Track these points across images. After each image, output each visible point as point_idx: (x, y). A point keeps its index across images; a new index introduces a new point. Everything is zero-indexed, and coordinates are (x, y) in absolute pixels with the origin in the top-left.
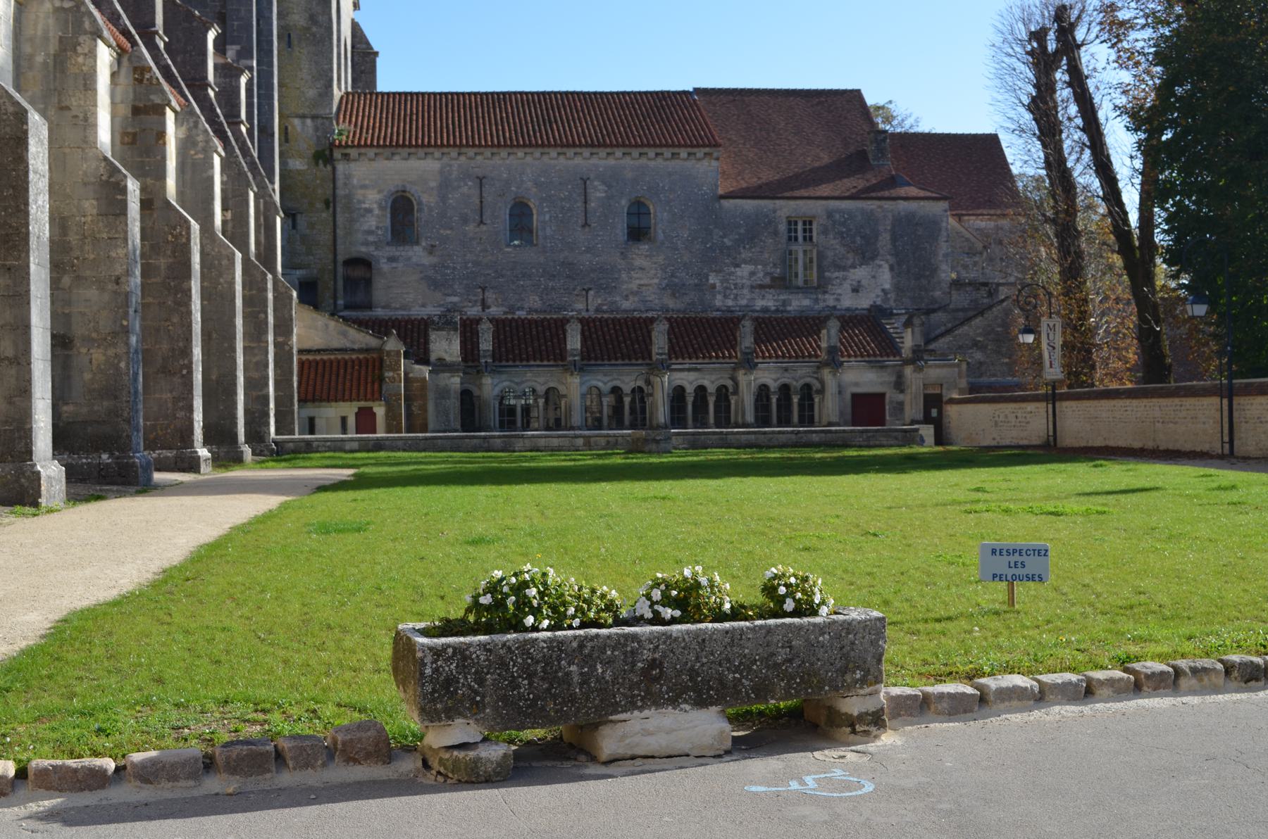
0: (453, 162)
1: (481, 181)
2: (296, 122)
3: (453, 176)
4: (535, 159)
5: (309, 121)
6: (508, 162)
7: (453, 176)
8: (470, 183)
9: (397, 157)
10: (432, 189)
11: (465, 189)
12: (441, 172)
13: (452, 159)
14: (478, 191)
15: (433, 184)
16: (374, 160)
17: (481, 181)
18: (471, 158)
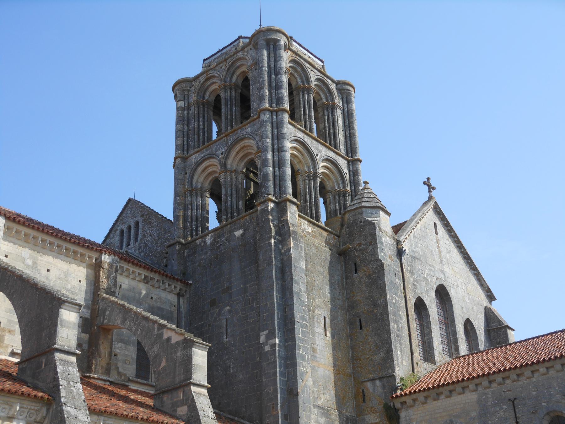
0: (487, 390)
1: (513, 401)
2: (369, 385)
3: (489, 403)
4: (558, 371)
5: (378, 382)
6: (534, 380)
7: (489, 403)
8: (504, 407)
9: (442, 397)
10: (474, 419)
11: (501, 414)
12: (479, 401)
13: (486, 388)
14: (513, 412)
15: (473, 414)
16: (425, 403)
17: (513, 401)
18: (500, 384)
